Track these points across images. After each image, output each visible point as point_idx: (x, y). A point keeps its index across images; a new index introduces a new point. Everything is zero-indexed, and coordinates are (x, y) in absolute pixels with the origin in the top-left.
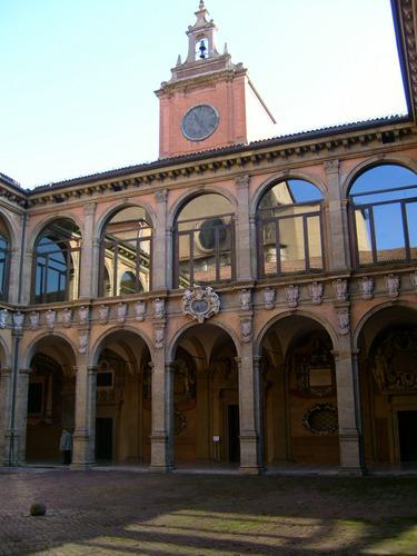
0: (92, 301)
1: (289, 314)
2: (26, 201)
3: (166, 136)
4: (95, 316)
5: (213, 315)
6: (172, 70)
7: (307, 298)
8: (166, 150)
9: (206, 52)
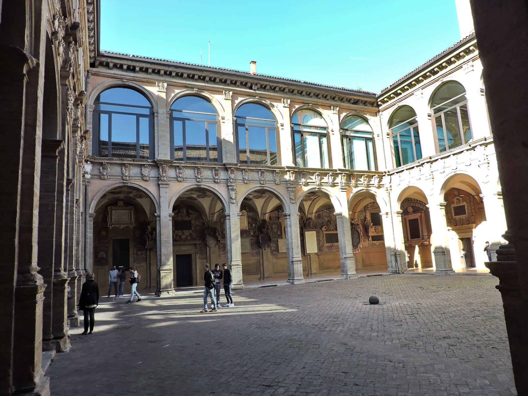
0: (431, 158)
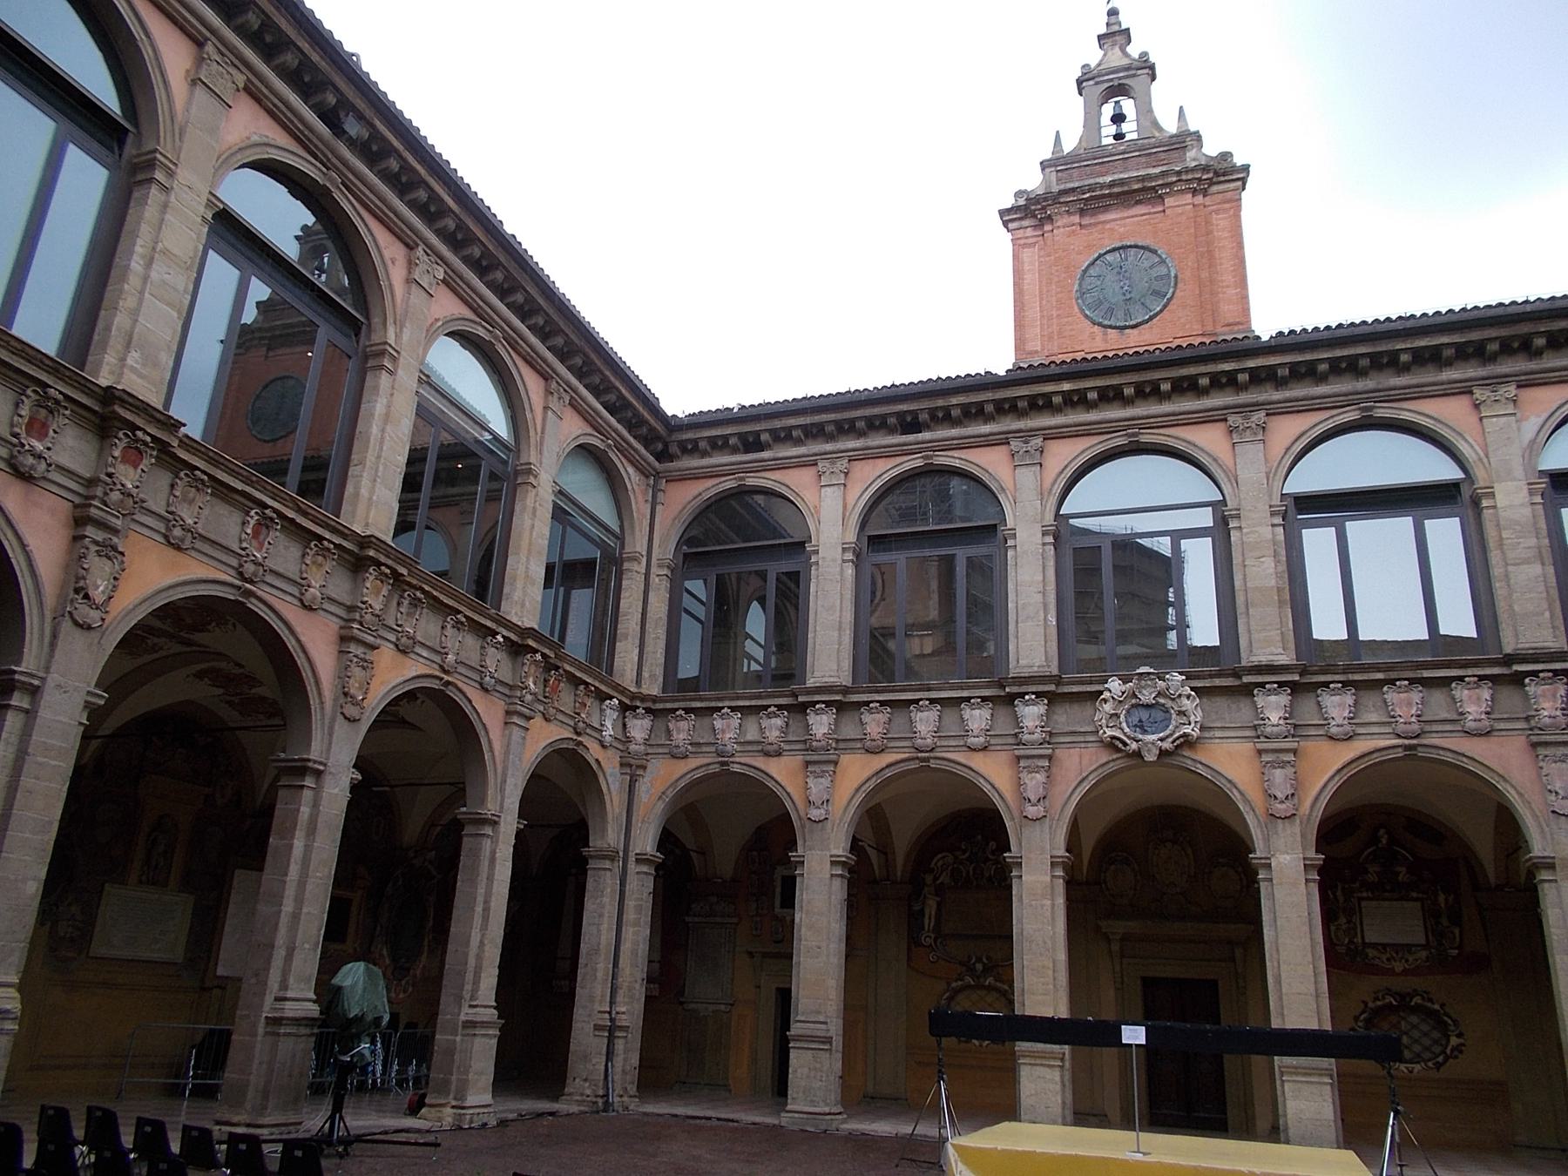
0: (846, 691)
1: (1400, 753)
2: (666, 445)
3: (1033, 312)
4: (849, 730)
5: (1187, 742)
6: (1044, 165)
7: (1444, 715)
8: (1034, 345)
9: (1125, 127)
